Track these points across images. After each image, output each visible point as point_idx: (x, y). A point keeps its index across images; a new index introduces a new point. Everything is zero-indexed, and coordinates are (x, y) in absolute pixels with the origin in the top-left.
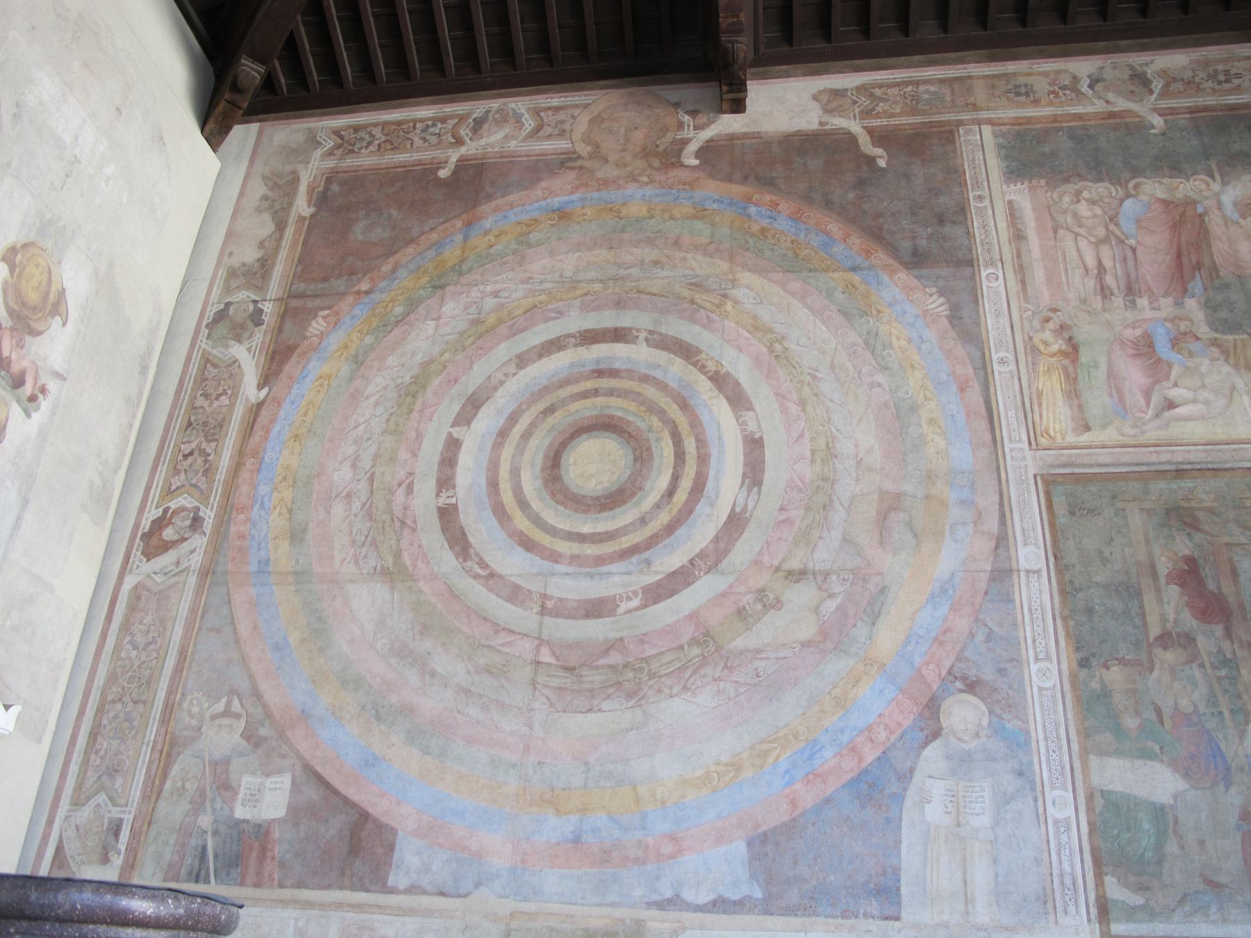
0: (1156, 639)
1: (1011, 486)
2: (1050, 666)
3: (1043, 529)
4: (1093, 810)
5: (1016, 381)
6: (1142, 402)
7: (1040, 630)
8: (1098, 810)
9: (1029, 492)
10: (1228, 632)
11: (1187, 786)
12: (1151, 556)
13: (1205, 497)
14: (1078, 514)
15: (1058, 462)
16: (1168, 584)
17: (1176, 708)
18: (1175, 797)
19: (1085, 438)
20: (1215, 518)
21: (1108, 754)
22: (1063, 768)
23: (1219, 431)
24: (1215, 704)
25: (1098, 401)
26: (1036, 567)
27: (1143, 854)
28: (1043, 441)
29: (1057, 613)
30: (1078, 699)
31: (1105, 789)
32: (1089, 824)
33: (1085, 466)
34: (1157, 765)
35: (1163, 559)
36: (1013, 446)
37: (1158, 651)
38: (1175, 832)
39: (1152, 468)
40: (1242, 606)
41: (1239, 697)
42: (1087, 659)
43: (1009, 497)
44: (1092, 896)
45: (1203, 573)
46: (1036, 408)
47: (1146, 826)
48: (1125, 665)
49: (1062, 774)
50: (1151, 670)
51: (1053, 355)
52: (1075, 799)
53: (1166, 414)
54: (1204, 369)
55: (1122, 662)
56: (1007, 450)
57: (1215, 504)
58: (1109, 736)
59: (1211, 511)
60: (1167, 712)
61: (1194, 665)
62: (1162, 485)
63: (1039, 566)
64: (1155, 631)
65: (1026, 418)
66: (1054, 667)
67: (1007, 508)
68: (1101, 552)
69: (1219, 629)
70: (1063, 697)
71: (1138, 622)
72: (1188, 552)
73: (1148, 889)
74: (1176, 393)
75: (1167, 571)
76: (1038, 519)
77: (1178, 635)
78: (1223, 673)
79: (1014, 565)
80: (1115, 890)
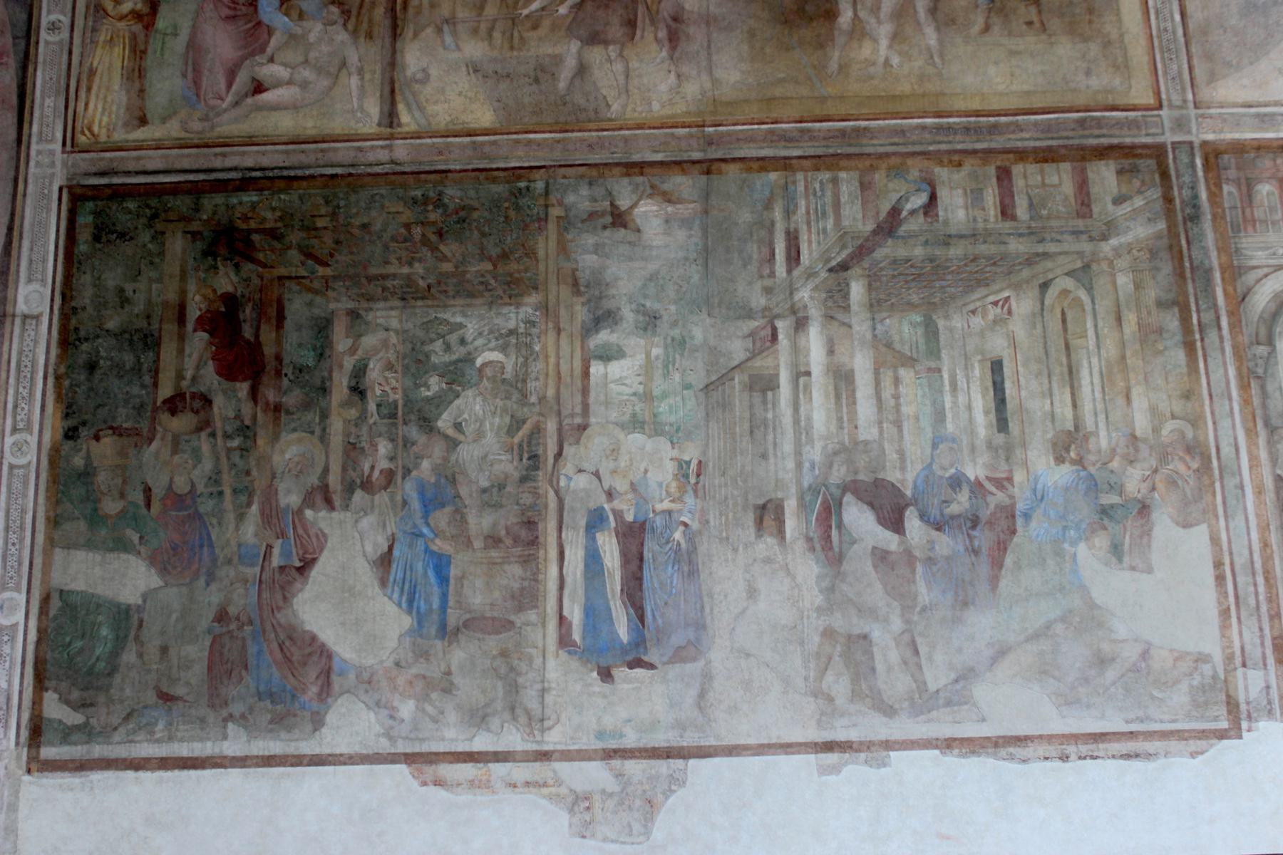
0: (164, 402)
1: (29, 201)
2: (29, 438)
3: (56, 260)
4: (47, 614)
5: (65, 57)
6: (223, 86)
7: (25, 393)
8: (52, 613)
9: (49, 210)
10: (254, 394)
12: (183, 292)
13: (269, 215)
14: (104, 239)
15: (94, 169)
16: (195, 330)
17: (170, 488)
18: (145, 597)
19: (140, 134)
20: (275, 243)
21: (76, 546)
22: (20, 564)
23: (310, 124)
24: (217, 482)
25: (166, 83)
26: (35, 312)
27: (94, 665)
28: (82, 139)
29: (51, 370)
30: (54, 479)
31: (66, 588)
32: (39, 631)
33: (128, 173)
34: (132, 558)
35: (198, 298)
36: (41, 147)
37: (164, 417)
38: (137, 638)
39: (213, 176)
40: (279, 358)
41: (248, 473)
42: (75, 429)
43: (23, 217)
44: (26, 716)
46: (83, 94)
47: (104, 631)
48: (120, 435)
49: (19, 572)
50: (150, 441)
51: (122, 18)
52: (28, 602)
53: (249, 100)
54: (312, 37)
55: (117, 431)
56: (33, 153)
57: (279, 224)
58: (82, 525)
59: (273, 234)
60: (158, 492)
61: (203, 435)
62: (219, 199)
63: (40, 309)
64: (165, 392)
65: (66, 107)
66: (33, 440)
67: (16, 233)
69: (243, 388)
70: (37, 477)
71: (147, 379)
72: (230, 289)
73: (92, 705)
74: (270, 71)
75: (198, 313)
76: (52, 248)
77: (193, 396)
78: (236, 443)
79: (9, 309)
80: (54, 708)
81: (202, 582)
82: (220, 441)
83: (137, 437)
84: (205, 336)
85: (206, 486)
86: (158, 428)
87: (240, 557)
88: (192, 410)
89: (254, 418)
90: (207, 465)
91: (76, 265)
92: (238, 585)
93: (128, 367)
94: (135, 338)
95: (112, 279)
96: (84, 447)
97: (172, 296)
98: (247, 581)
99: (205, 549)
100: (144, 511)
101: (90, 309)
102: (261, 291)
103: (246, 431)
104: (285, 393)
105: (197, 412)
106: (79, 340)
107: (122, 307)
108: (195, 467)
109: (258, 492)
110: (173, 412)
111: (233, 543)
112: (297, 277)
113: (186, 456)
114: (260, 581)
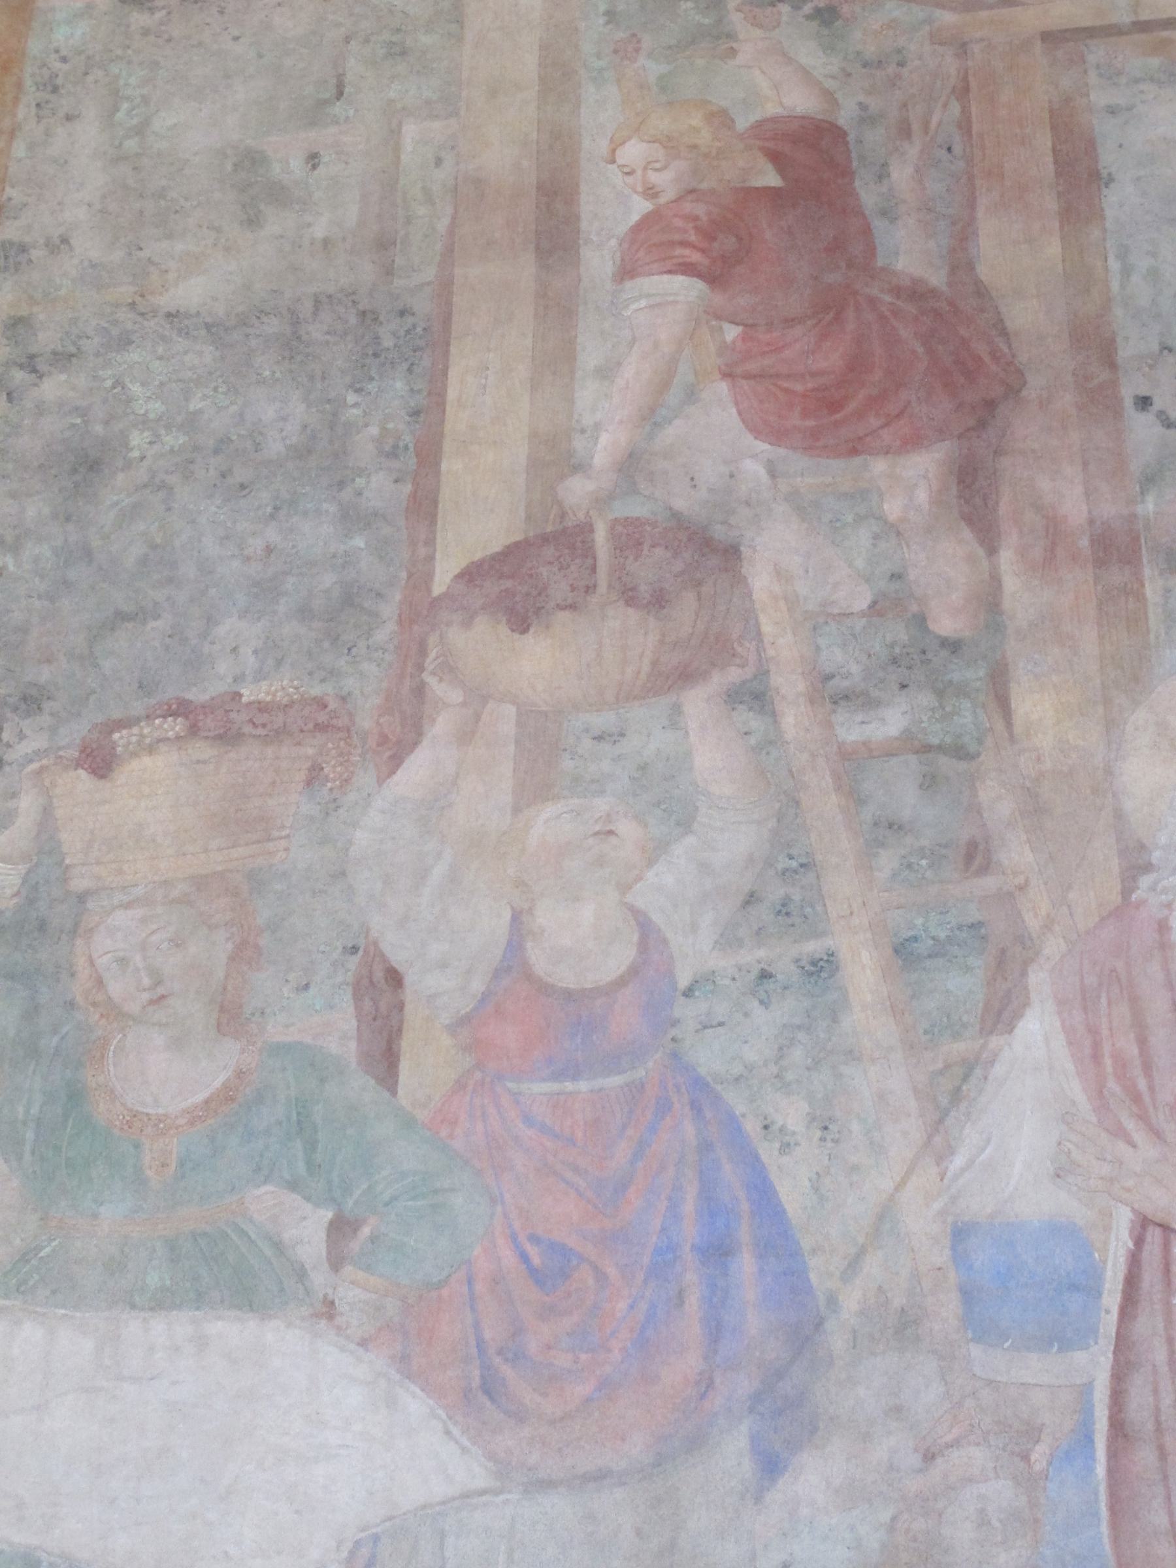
0: (471, 575)
10: (972, 496)
11: (468, 1470)
16: (626, 272)
17: (513, 961)
37: (477, 641)
40: (1094, 342)
41: (976, 856)
45: (868, 196)
48: (228, 737)
50: (394, 753)
55: (213, 723)
60: (441, 985)
61: (698, 702)
64: (480, 518)
68: (252, 159)
69: (910, 481)
71: (380, 489)
72: (800, 101)
75: (641, 207)
77: (631, 536)
78: (892, 722)
81: (733, 1452)
82: (794, 719)
83: (337, 741)
84: (685, 289)
85: (728, 940)
86: (437, 687)
87: (968, 1295)
88: (629, 596)
89: (989, 602)
90: (731, 838)
91: (31, 95)
92: (976, 1456)
93: (275, 447)
94: (315, 331)
95: (193, 130)
96: (28, 803)
97: (502, 148)
98: (1033, 1432)
99: (746, 1264)
100: (360, 1086)
101: (89, 247)
102: (963, 91)
103: (943, 665)
104: (1150, 480)
105: (659, 601)
106: (30, 364)
107: (253, 222)
108: (654, 852)
109: (1053, 947)
110: (522, 617)
111: (921, 1222)
112: (1143, 27)
113: (602, 805)
114: (1119, 1427)
